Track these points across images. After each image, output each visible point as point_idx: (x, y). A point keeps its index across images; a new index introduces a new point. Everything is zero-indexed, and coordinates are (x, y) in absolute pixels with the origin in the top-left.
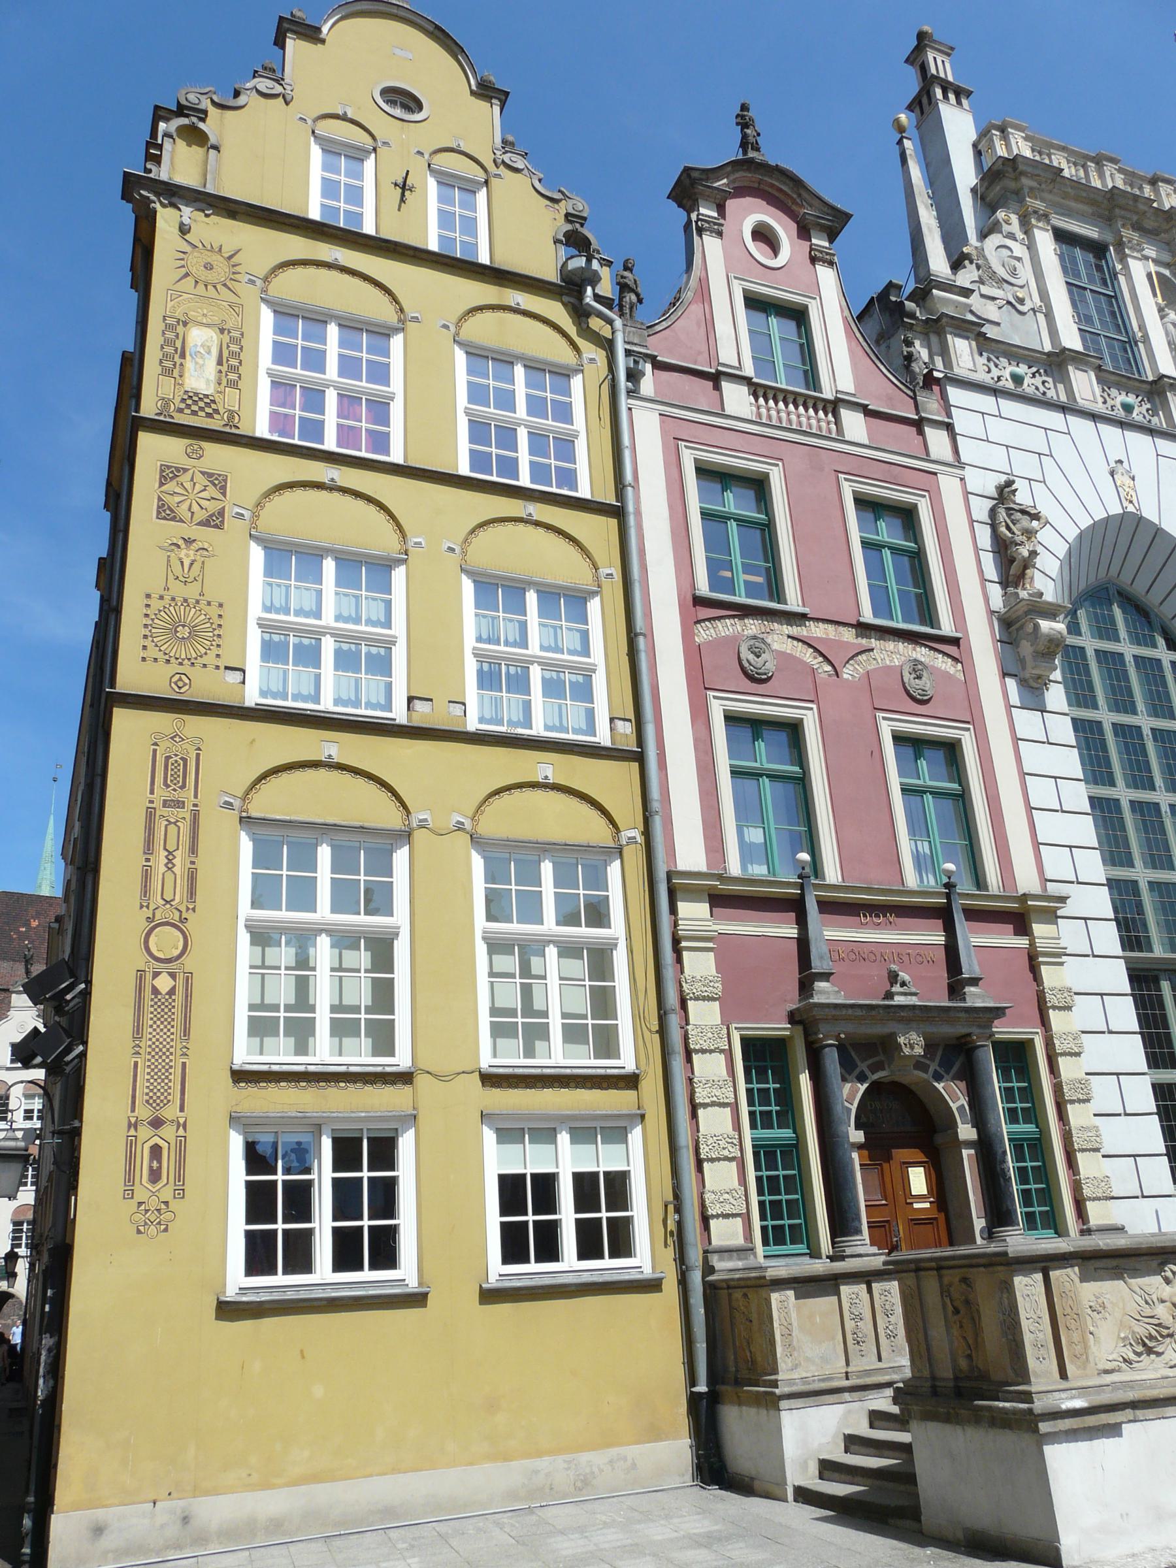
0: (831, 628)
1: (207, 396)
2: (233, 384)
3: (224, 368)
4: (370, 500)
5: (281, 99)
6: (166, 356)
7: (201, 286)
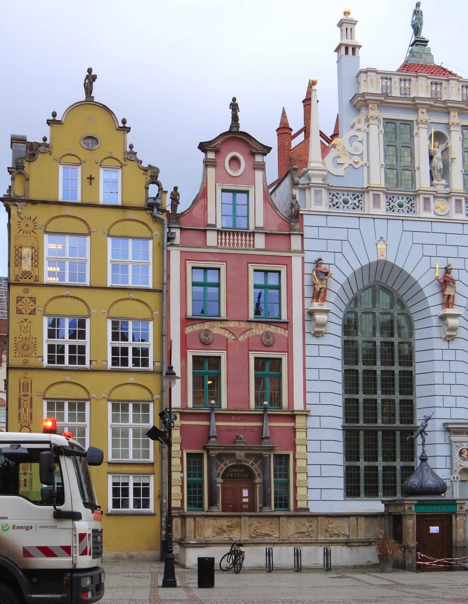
0: (237, 324)
1: (29, 272)
2: (36, 266)
3: (33, 261)
4: (79, 299)
5: (48, 153)
6: (16, 260)
7: (25, 233)
